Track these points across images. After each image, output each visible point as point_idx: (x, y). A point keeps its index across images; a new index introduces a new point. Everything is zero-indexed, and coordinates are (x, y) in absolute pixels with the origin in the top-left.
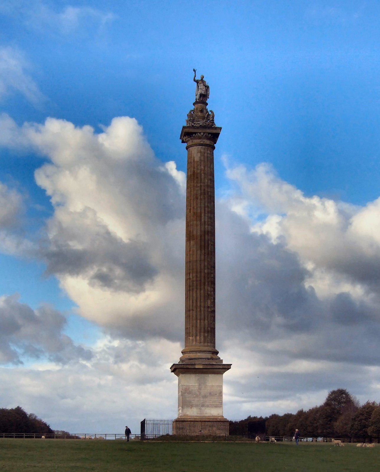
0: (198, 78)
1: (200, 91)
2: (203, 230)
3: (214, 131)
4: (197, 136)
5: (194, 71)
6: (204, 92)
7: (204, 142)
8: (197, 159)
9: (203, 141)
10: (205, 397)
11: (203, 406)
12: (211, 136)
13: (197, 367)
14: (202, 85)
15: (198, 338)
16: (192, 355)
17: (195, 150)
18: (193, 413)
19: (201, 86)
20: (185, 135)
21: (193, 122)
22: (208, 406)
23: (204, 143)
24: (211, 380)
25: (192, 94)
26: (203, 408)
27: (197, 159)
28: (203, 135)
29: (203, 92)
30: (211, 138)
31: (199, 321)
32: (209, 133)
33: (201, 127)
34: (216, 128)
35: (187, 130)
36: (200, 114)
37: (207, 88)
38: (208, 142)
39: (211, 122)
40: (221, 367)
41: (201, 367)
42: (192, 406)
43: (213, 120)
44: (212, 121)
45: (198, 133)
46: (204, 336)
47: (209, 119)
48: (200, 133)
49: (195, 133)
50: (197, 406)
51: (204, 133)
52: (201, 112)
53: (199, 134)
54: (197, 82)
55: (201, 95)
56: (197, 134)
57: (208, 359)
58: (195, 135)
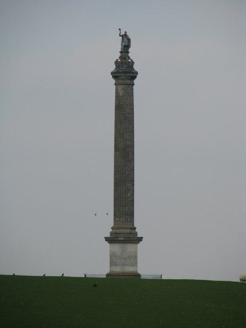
0: (123, 33)
1: (124, 44)
2: (124, 144)
3: (133, 75)
5: (120, 29)
8: (121, 94)
10: (125, 259)
11: (124, 265)
13: (119, 239)
15: (121, 219)
16: (117, 231)
17: (120, 87)
18: (118, 269)
19: (125, 39)
22: (127, 265)
24: (130, 247)
25: (118, 47)
26: (124, 267)
27: (121, 94)
29: (126, 44)
31: (122, 208)
33: (124, 72)
34: (134, 73)
37: (129, 40)
38: (128, 82)
40: (136, 239)
41: (122, 239)
42: (117, 265)
43: (132, 66)
46: (125, 218)
50: (120, 265)
54: (122, 36)
55: (125, 46)
57: (128, 233)
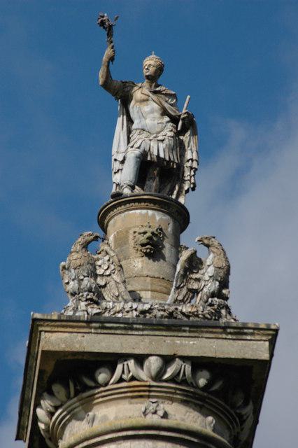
4: (121, 380)
6: (162, 146)
7: (165, 416)
9: (161, 413)
12: (210, 383)
14: (152, 112)
20: (46, 389)
21: (97, 303)
23: (165, 422)
28: (162, 371)
29: (160, 149)
30: (216, 393)
32: (199, 363)
33: (146, 323)
35: (54, 340)
36: (138, 264)
39: (211, 305)
44: (213, 295)
45: (125, 357)
47: (195, 286)
48: (140, 359)
49: (111, 361)
51: (167, 360)
52: (148, 255)
53: (131, 363)
56: (119, 367)
58: (113, 371)
